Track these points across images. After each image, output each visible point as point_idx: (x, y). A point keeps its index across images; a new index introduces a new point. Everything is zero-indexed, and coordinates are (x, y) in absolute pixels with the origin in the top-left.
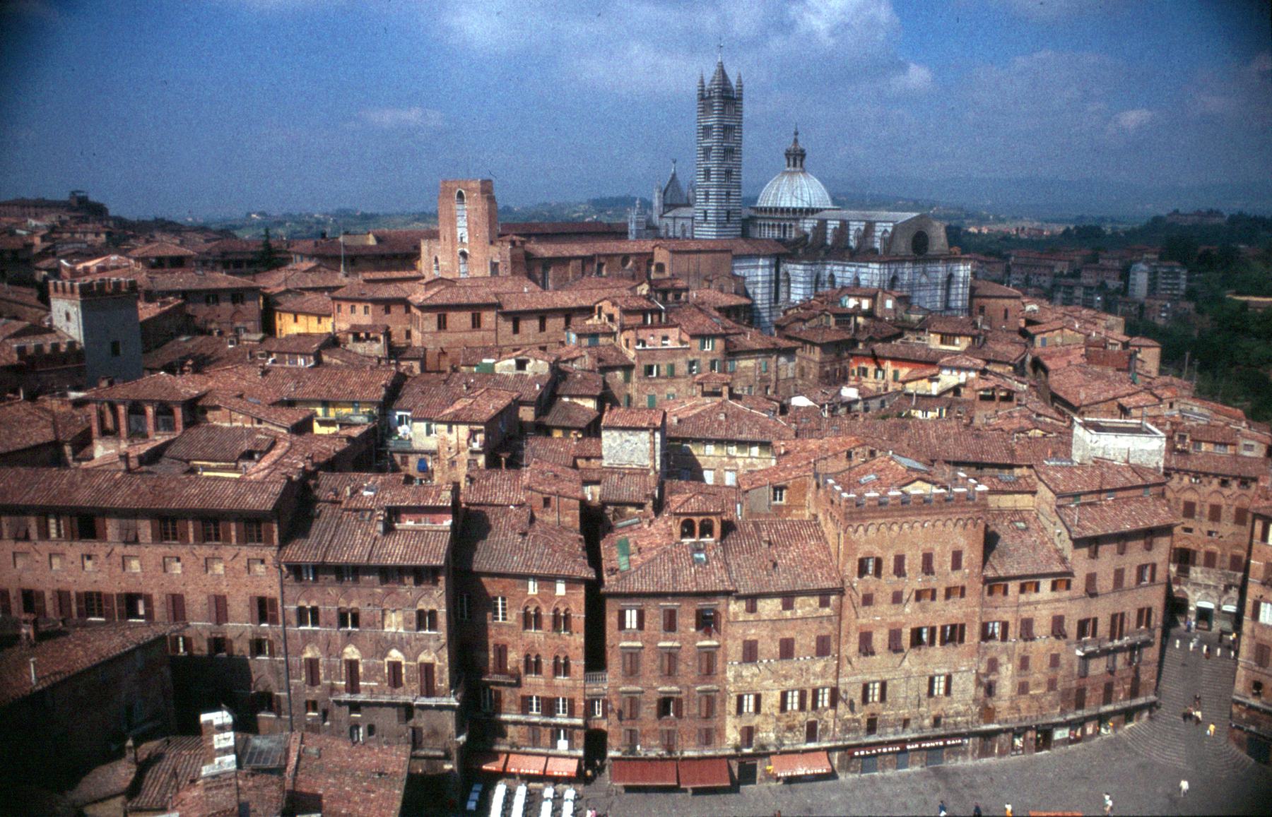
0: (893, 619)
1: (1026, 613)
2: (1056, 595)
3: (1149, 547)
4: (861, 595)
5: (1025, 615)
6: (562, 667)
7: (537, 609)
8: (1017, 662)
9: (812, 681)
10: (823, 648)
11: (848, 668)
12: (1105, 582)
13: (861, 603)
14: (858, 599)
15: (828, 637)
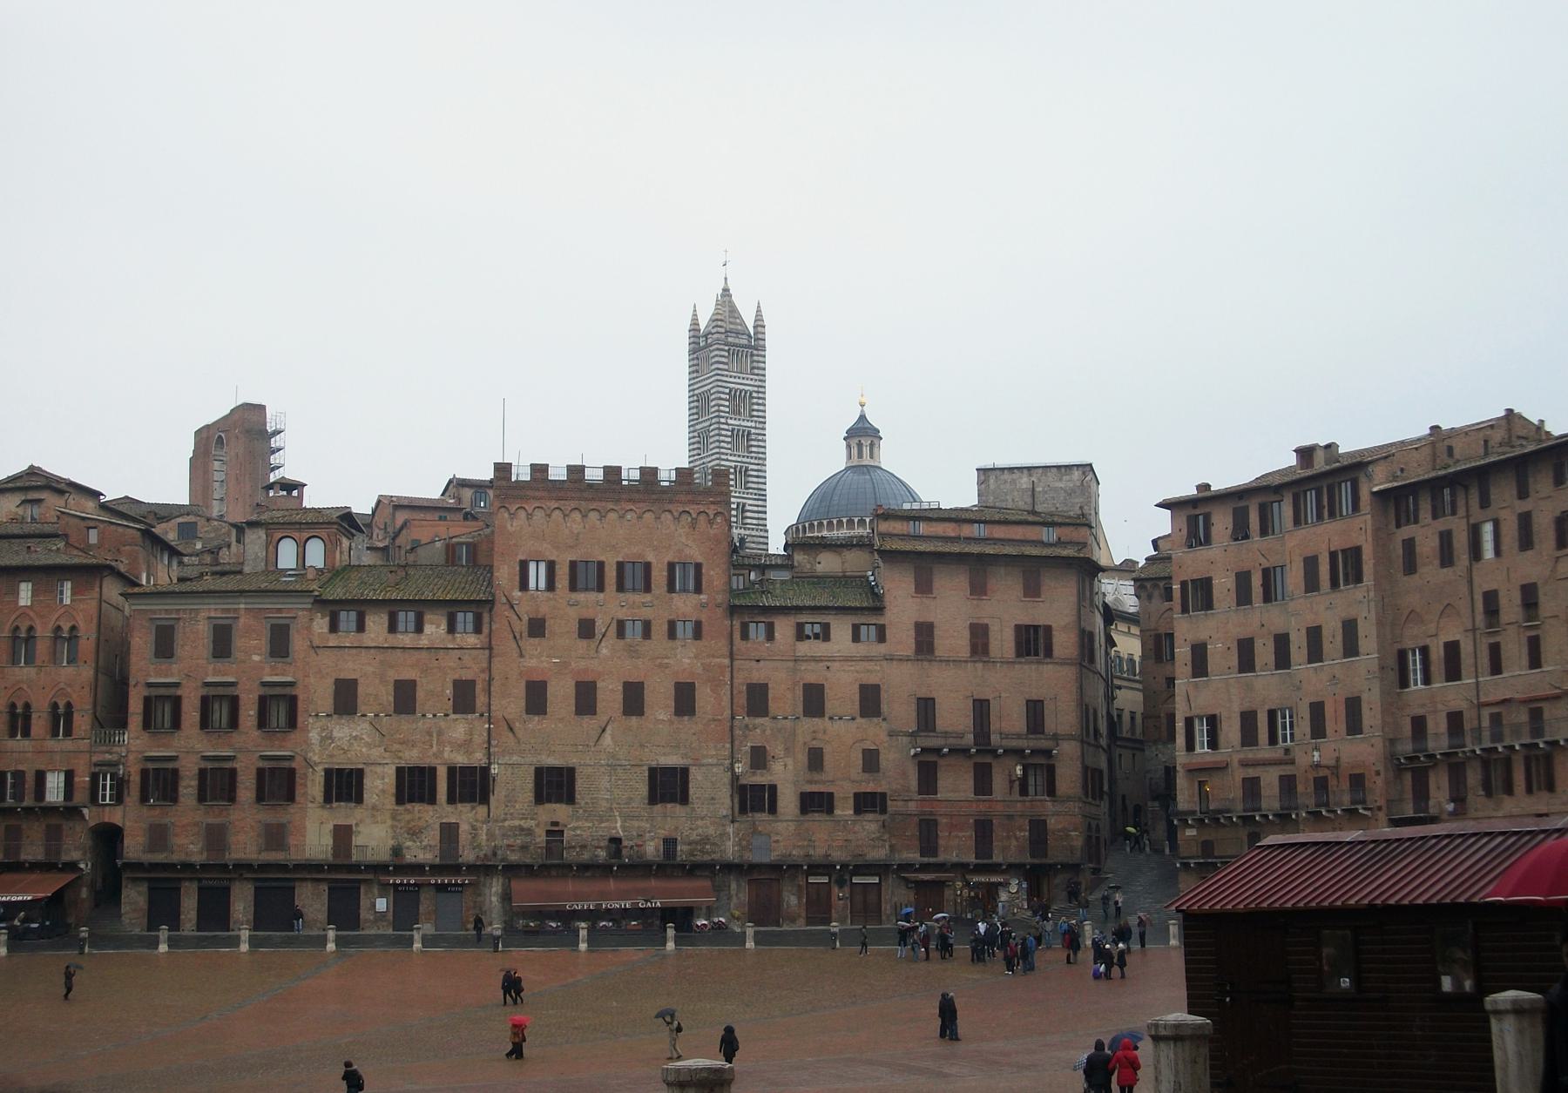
0: (583, 664)
1: (812, 674)
2: (860, 649)
3: (1032, 590)
4: (525, 618)
5: (811, 678)
6: (62, 720)
7: (31, 628)
8: (803, 758)
9: (446, 755)
10: (464, 698)
11: (508, 739)
12: (952, 639)
13: (525, 634)
14: (522, 627)
15: (473, 682)
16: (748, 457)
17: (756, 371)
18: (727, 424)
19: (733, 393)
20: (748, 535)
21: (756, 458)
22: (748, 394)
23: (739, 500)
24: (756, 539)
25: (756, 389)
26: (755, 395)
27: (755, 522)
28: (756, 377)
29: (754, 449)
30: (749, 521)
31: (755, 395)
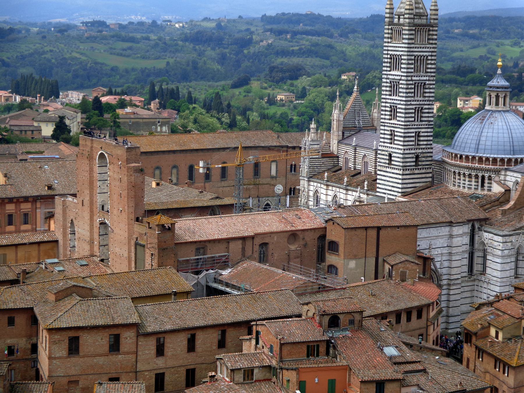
16: (423, 101)
17: (431, 42)
18: (412, 80)
19: (416, 58)
20: (421, 153)
21: (428, 101)
22: (425, 58)
23: (416, 130)
24: (425, 155)
25: (430, 54)
26: (429, 58)
27: (425, 143)
28: (431, 46)
29: (427, 95)
30: (422, 143)
31: (429, 58)
